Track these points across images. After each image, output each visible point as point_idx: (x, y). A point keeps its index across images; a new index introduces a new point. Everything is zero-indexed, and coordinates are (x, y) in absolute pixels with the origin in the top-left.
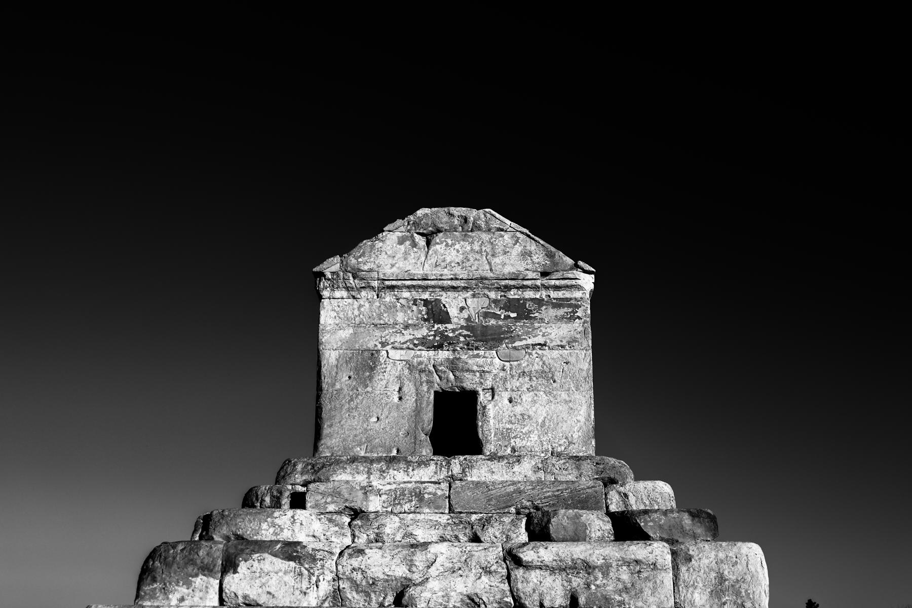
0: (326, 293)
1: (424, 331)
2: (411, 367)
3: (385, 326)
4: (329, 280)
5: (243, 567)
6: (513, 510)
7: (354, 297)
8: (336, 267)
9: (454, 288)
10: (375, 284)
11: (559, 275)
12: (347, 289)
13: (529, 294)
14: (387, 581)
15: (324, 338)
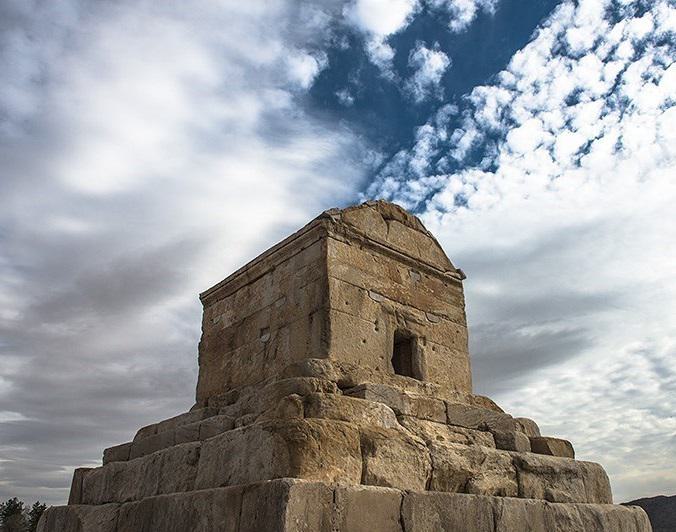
0: (331, 234)
1: (388, 285)
2: (386, 311)
3: (366, 271)
4: (334, 224)
5: (379, 453)
6: (476, 427)
7: (347, 243)
8: (338, 217)
9: (404, 261)
10: (362, 238)
11: (453, 274)
12: (345, 235)
13: (439, 281)
14: (459, 474)
15: (331, 267)
